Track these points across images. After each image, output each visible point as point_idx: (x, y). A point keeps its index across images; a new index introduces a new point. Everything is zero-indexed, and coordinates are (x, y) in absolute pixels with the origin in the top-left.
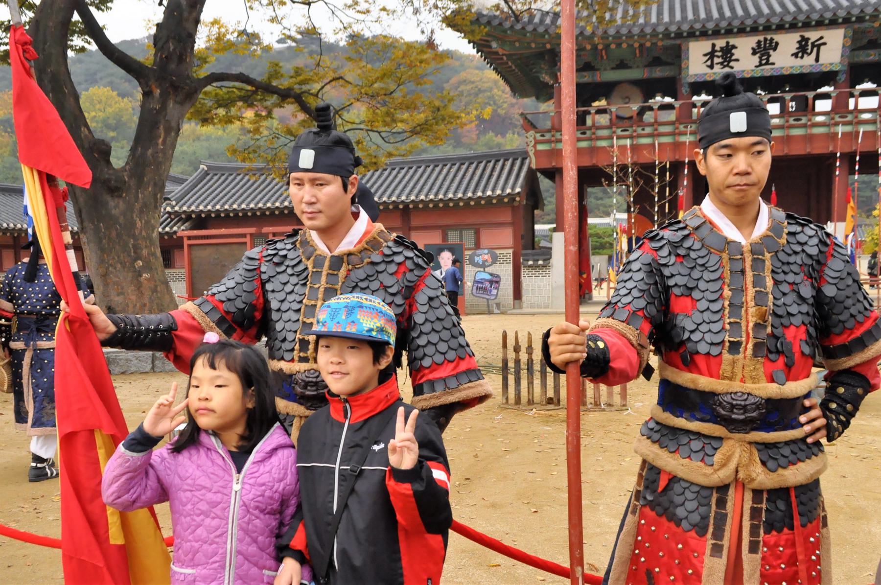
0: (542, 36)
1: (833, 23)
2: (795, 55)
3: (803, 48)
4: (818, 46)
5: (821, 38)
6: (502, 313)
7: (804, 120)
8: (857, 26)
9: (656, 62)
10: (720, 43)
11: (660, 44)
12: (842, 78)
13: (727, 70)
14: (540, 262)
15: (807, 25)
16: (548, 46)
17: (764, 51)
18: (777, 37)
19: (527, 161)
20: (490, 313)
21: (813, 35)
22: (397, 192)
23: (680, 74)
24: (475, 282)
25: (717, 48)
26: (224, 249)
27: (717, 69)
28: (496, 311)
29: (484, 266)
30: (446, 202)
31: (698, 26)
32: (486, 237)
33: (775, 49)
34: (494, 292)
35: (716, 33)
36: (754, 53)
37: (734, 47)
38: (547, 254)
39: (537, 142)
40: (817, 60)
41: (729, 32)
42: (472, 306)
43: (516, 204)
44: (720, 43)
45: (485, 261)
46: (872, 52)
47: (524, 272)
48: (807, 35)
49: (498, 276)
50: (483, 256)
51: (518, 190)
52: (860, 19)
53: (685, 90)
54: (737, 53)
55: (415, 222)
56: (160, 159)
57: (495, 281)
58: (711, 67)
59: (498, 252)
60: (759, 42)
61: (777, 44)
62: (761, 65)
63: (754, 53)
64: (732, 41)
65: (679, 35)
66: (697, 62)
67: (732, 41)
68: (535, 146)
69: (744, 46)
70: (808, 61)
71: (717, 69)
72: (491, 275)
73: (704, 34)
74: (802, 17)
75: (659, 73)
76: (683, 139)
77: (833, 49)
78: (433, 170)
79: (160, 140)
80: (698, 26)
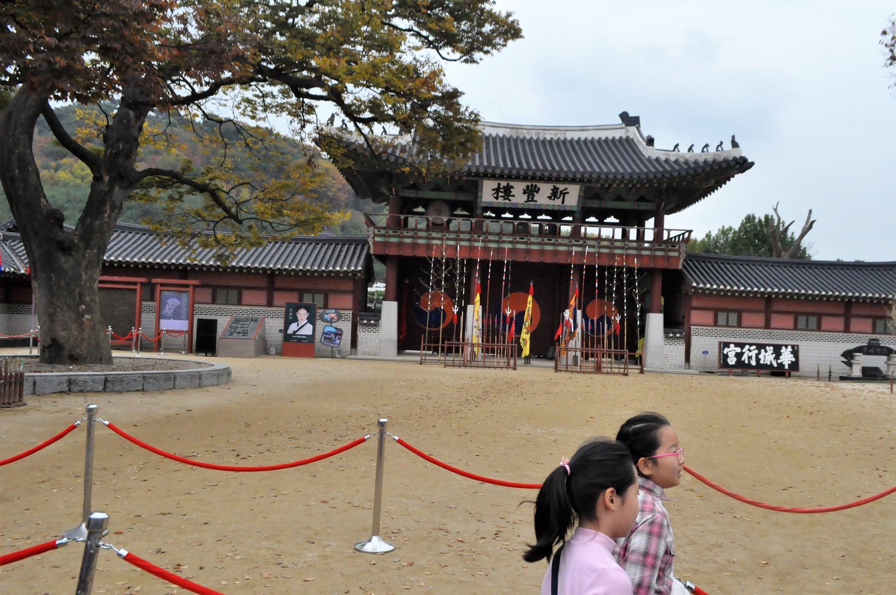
0: (385, 161)
1: (573, 181)
2: (550, 198)
3: (555, 194)
4: (564, 193)
6: (342, 358)
7: (553, 241)
8: (588, 185)
9: (460, 189)
10: (504, 183)
11: (464, 178)
12: (578, 216)
13: (507, 201)
14: (372, 322)
15: (558, 180)
16: (388, 169)
17: (531, 192)
18: (539, 185)
19: (366, 247)
20: (333, 357)
21: (561, 187)
22: (266, 261)
23: (476, 198)
24: (324, 333)
25: (501, 186)
27: (500, 200)
28: (338, 356)
29: (331, 321)
30: (305, 272)
31: (490, 171)
32: (333, 300)
33: (537, 192)
34: (338, 341)
35: (501, 177)
36: (524, 193)
37: (512, 187)
38: (376, 314)
39: (375, 235)
40: (563, 202)
41: (509, 177)
42: (319, 351)
43: (357, 278)
44: (504, 183)
45: (332, 319)
46: (595, 201)
47: (360, 329)
48: (557, 186)
49: (341, 330)
50: (331, 314)
51: (360, 268)
52: (590, 181)
53: (479, 211)
54: (514, 192)
56: (105, 229)
57: (339, 333)
58: (497, 198)
59: (342, 312)
60: (528, 186)
61: (539, 189)
62: (528, 201)
63: (524, 193)
64: (511, 183)
65: (477, 174)
66: (488, 193)
67: (511, 183)
68: (373, 238)
69: (518, 188)
70: (558, 202)
71: (500, 200)
72: (336, 329)
73: (493, 176)
74: (555, 175)
75: (462, 197)
76: (476, 244)
77: (573, 197)
78: (294, 247)
79: (106, 215)
80: (490, 171)
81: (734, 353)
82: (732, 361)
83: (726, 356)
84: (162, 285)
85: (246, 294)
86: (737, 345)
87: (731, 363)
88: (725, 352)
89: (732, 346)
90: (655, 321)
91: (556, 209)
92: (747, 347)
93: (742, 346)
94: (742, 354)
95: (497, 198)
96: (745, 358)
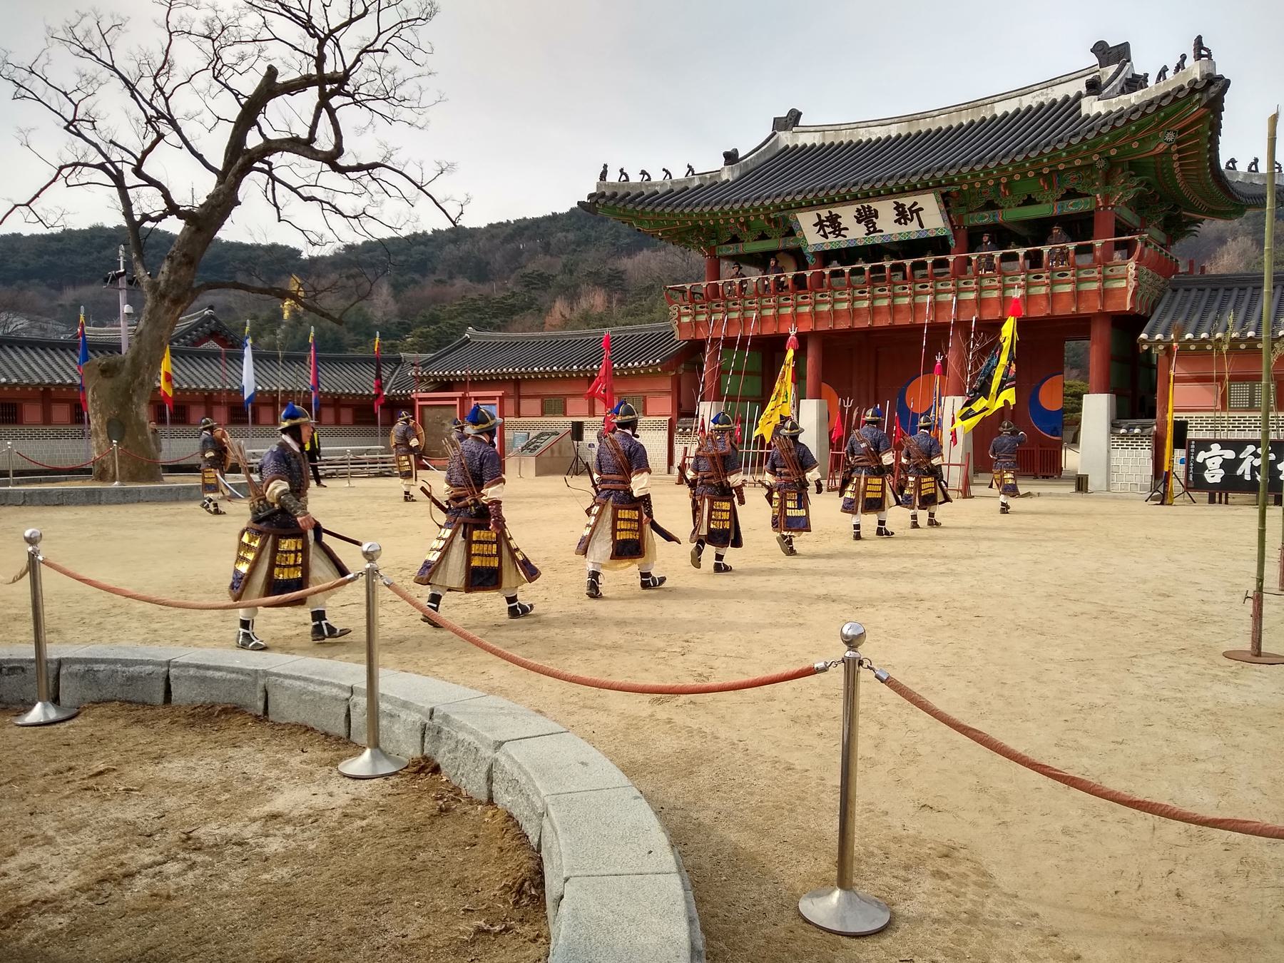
1: (926, 188)
3: (903, 215)
5: (915, 204)
10: (824, 213)
13: (840, 238)
15: (902, 191)
17: (867, 217)
21: (907, 201)
26: (444, 410)
35: (821, 204)
36: (859, 222)
40: (922, 226)
41: (832, 202)
44: (824, 213)
46: (985, 214)
48: (901, 201)
54: (844, 222)
55: (523, 391)
60: (858, 210)
62: (870, 233)
63: (859, 222)
64: (835, 211)
68: (679, 319)
69: (847, 215)
70: (913, 226)
71: (831, 238)
81: (1219, 461)
82: (1214, 475)
83: (1203, 467)
84: (476, 398)
85: (570, 402)
86: (1225, 444)
87: (1210, 480)
88: (1200, 459)
89: (1216, 448)
90: (1096, 409)
91: (914, 237)
92: (1251, 448)
93: (1238, 446)
94: (1238, 462)
95: (825, 236)
96: (1244, 469)
